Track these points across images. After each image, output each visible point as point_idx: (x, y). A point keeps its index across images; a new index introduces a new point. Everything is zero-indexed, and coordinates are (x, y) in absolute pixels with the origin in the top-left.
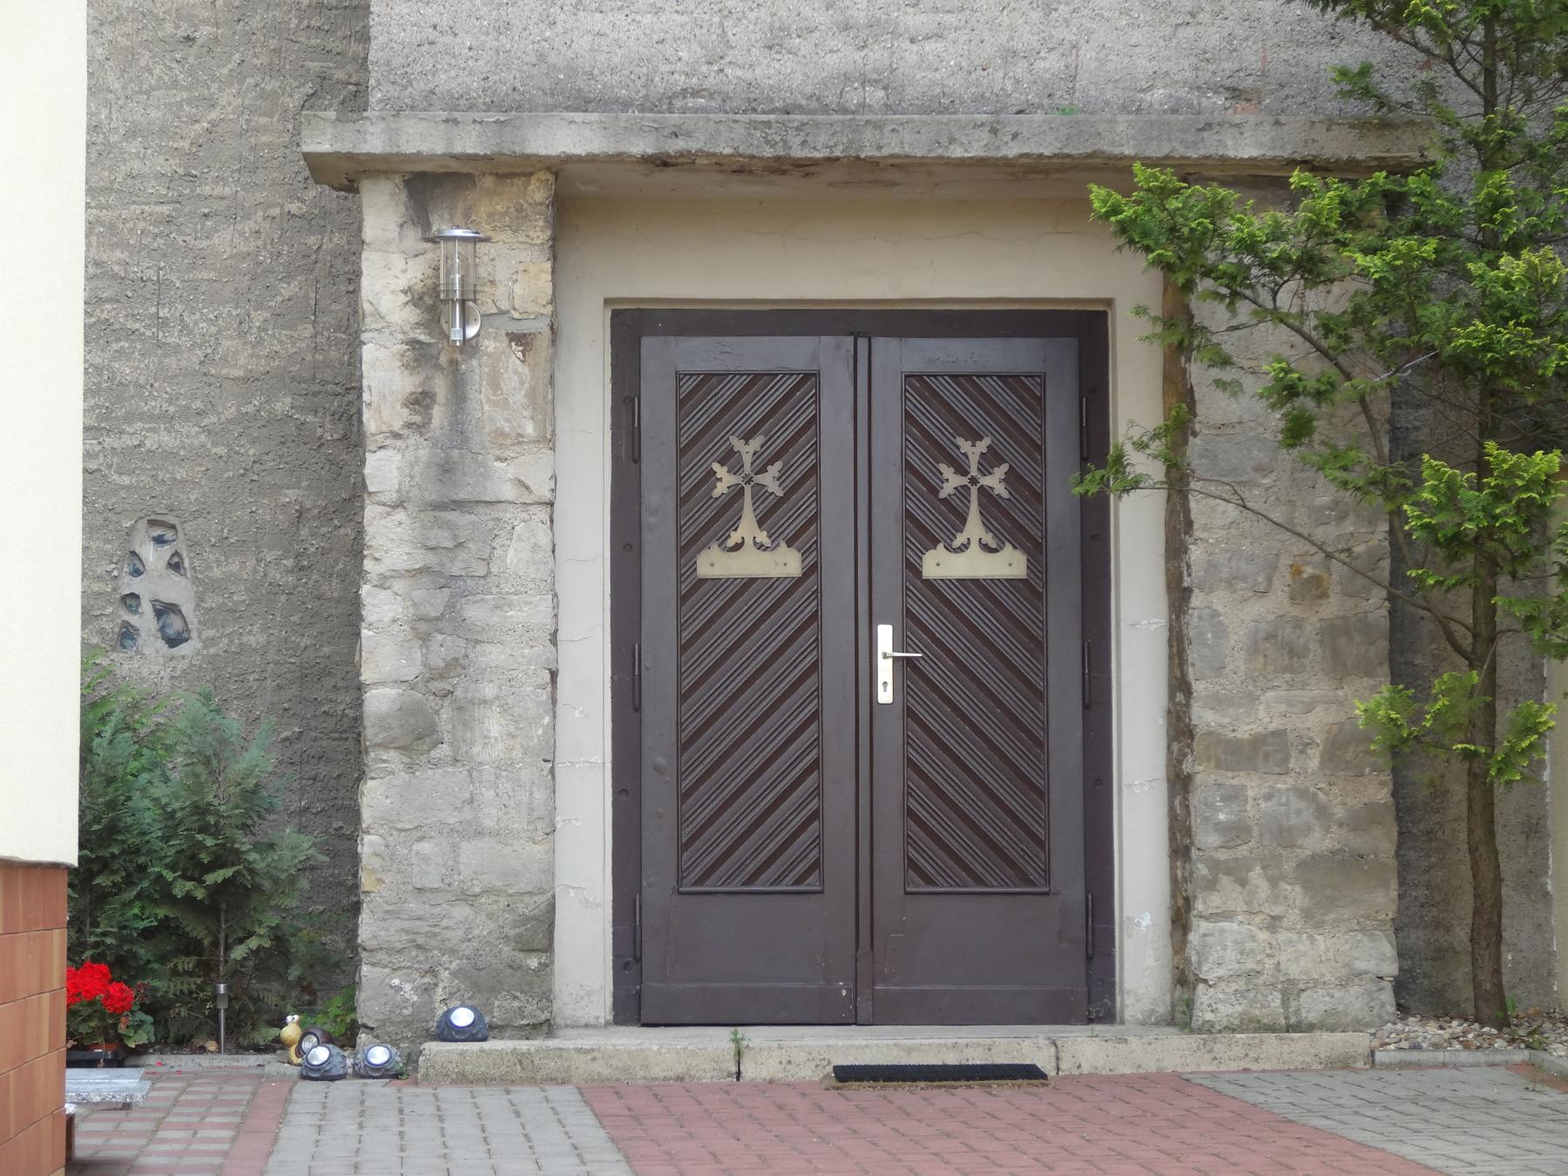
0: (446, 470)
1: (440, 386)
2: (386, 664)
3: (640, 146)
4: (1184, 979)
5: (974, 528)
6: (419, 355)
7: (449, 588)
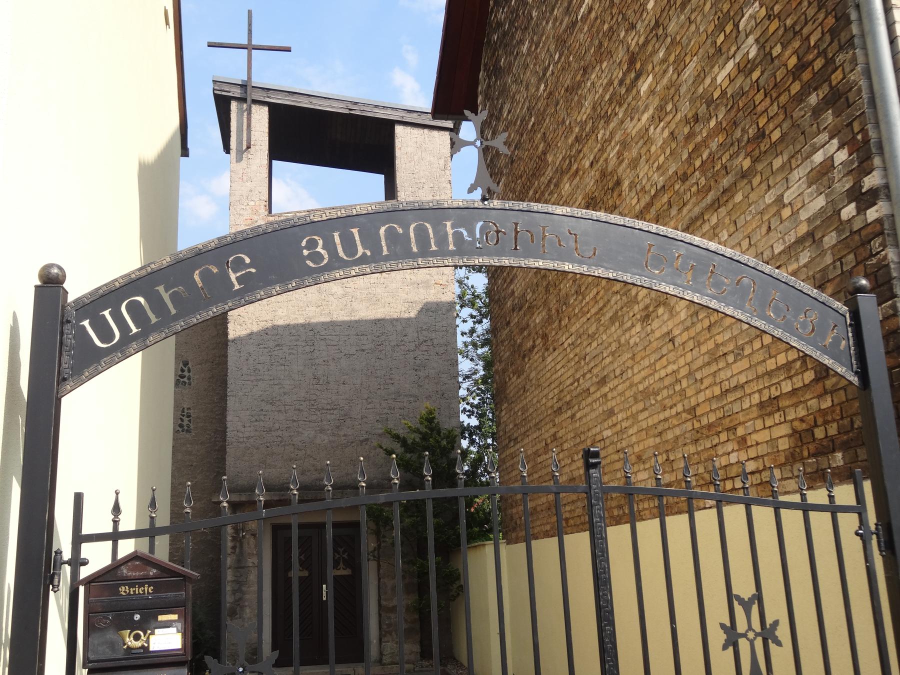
0: (239, 561)
1: (238, 545)
2: (229, 599)
3: (276, 498)
4: (381, 654)
5: (341, 565)
6: (234, 539)
7: (239, 583)
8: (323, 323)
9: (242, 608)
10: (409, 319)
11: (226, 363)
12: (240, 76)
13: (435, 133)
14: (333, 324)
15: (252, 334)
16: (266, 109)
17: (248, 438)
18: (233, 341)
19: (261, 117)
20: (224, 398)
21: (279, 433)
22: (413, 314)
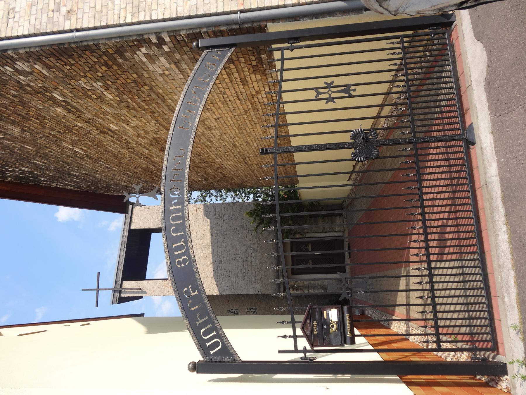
0: (306, 287)
2: (320, 291)
4: (340, 231)
5: (307, 247)
6: (298, 290)
7: (315, 287)
8: (213, 257)
9: (324, 285)
10: (211, 222)
11: (229, 295)
12: (110, 293)
13: (134, 212)
14: (213, 253)
15: (217, 285)
16: (124, 282)
17: (258, 285)
18: (220, 293)
19: (127, 284)
20: (243, 296)
21: (256, 273)
22: (209, 221)
